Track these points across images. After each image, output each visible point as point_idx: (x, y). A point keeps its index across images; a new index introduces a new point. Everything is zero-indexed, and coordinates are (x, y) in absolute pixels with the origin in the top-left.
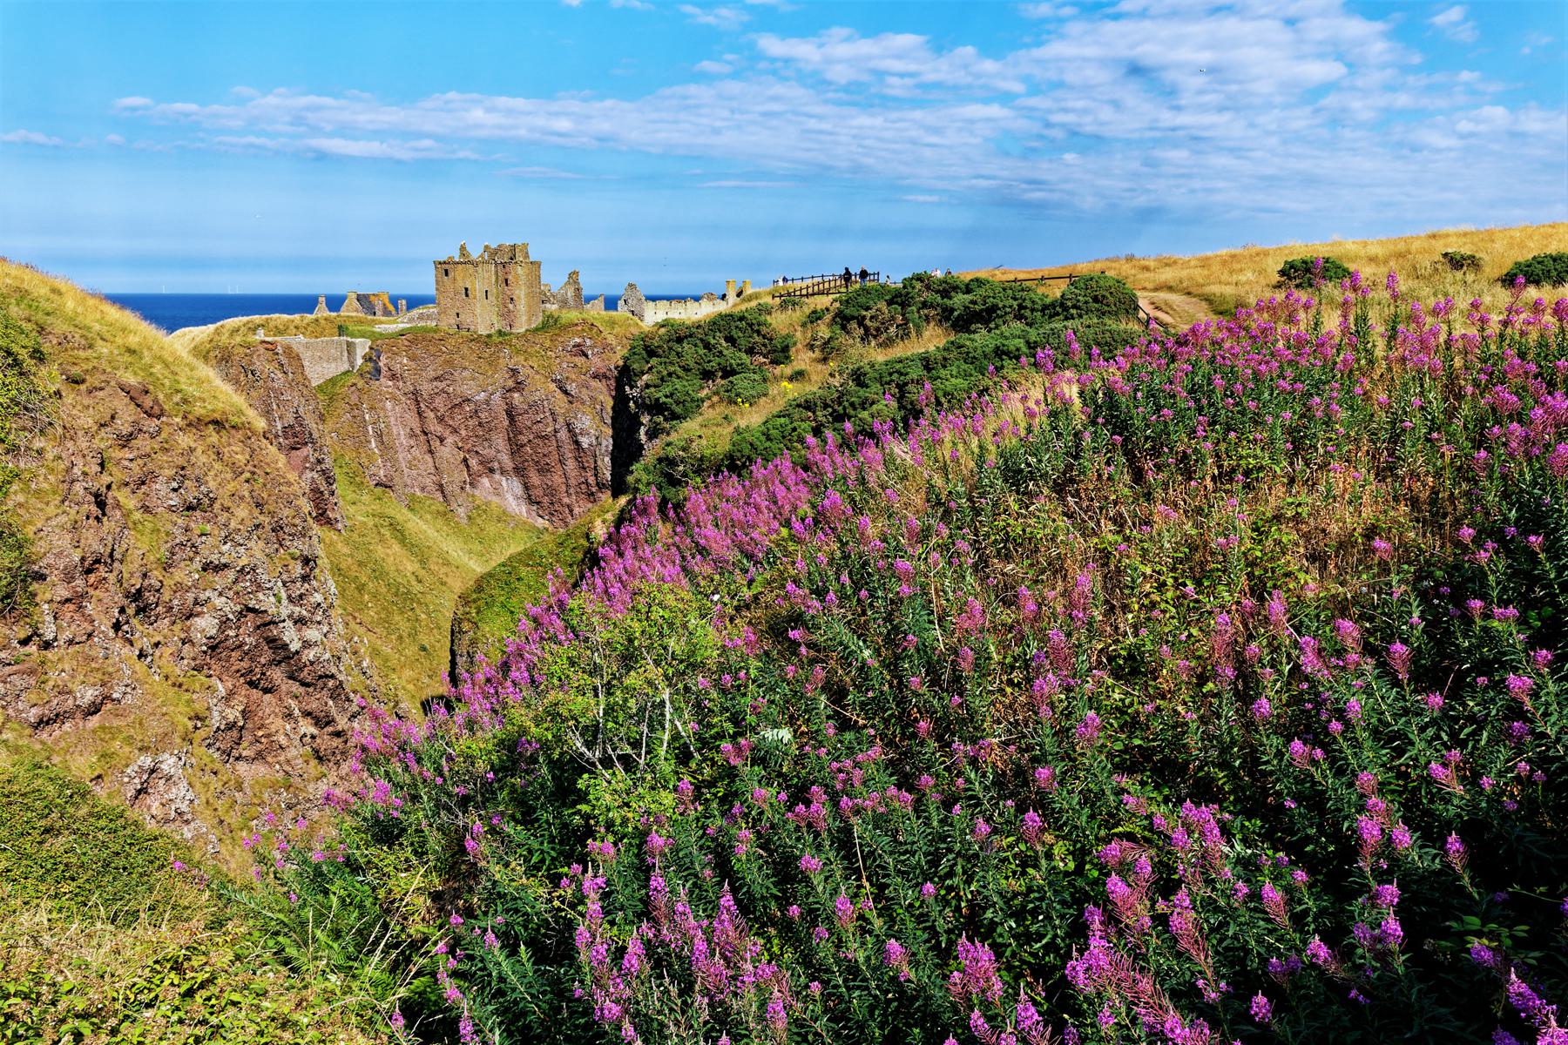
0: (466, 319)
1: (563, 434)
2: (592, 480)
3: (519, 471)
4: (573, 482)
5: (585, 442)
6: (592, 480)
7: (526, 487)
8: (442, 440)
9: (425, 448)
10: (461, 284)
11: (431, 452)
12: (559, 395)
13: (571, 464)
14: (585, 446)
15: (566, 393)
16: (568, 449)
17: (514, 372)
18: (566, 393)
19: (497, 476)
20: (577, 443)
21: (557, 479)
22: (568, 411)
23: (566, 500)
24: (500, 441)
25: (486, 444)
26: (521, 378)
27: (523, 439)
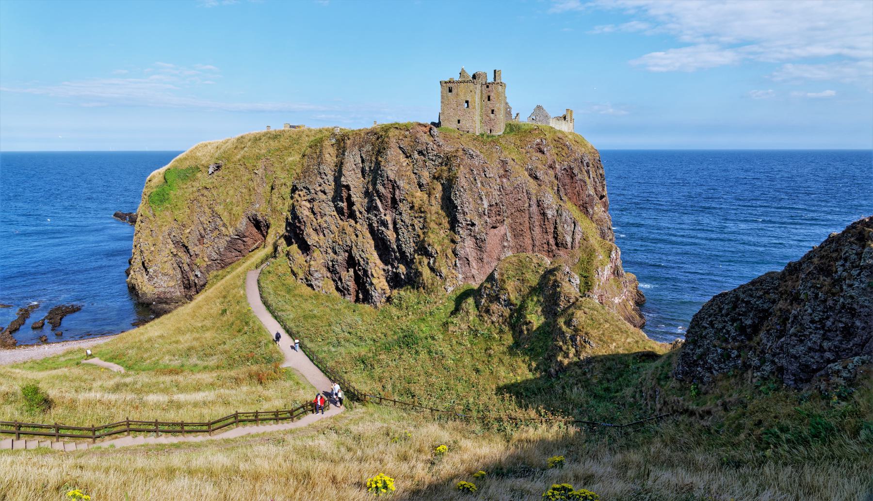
0: (466, 124)
1: (534, 208)
2: (552, 241)
4: (537, 243)
5: (550, 213)
10: (463, 98)
12: (531, 180)
13: (537, 230)
14: (550, 216)
15: (536, 178)
16: (537, 218)
17: (504, 163)
18: (536, 178)
20: (544, 214)
21: (528, 241)
22: (539, 191)
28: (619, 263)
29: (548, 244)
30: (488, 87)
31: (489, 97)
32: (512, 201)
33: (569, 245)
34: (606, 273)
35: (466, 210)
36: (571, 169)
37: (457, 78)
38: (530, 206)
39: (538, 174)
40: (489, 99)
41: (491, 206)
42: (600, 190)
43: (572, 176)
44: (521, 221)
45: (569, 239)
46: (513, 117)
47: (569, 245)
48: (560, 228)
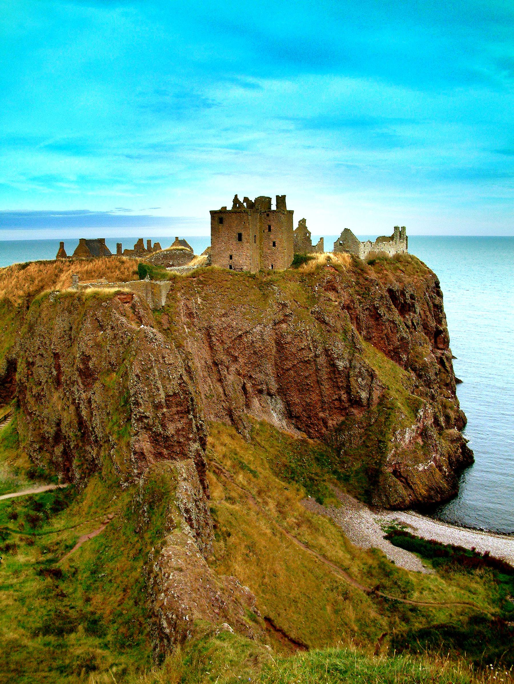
1: (322, 360)
2: (344, 397)
3: (282, 392)
5: (341, 364)
6: (344, 397)
7: (288, 405)
8: (228, 368)
9: (215, 377)
11: (220, 380)
14: (341, 368)
19: (265, 397)
21: (315, 397)
23: (321, 415)
24: (269, 368)
25: (258, 370)
26: (288, 311)
27: (288, 364)
28: (430, 421)
29: (340, 399)
30: (268, 215)
31: (270, 227)
32: (294, 350)
33: (365, 402)
34: (407, 436)
35: (140, 401)
36: (376, 309)
37: (229, 208)
38: (316, 356)
39: (327, 319)
40: (270, 230)
41: (168, 396)
42: (433, 324)
43: (377, 317)
44: (307, 374)
45: (364, 395)
46: (314, 243)
47: (365, 402)
48: (353, 383)
